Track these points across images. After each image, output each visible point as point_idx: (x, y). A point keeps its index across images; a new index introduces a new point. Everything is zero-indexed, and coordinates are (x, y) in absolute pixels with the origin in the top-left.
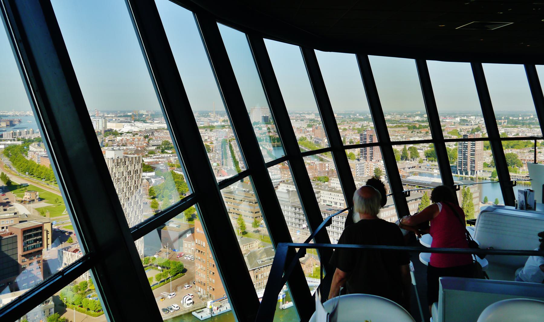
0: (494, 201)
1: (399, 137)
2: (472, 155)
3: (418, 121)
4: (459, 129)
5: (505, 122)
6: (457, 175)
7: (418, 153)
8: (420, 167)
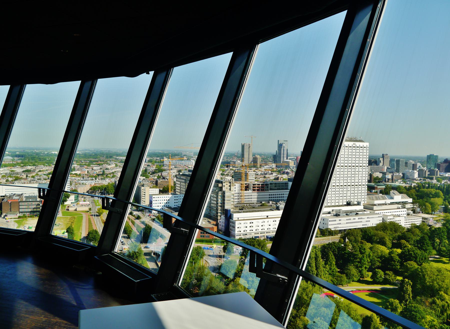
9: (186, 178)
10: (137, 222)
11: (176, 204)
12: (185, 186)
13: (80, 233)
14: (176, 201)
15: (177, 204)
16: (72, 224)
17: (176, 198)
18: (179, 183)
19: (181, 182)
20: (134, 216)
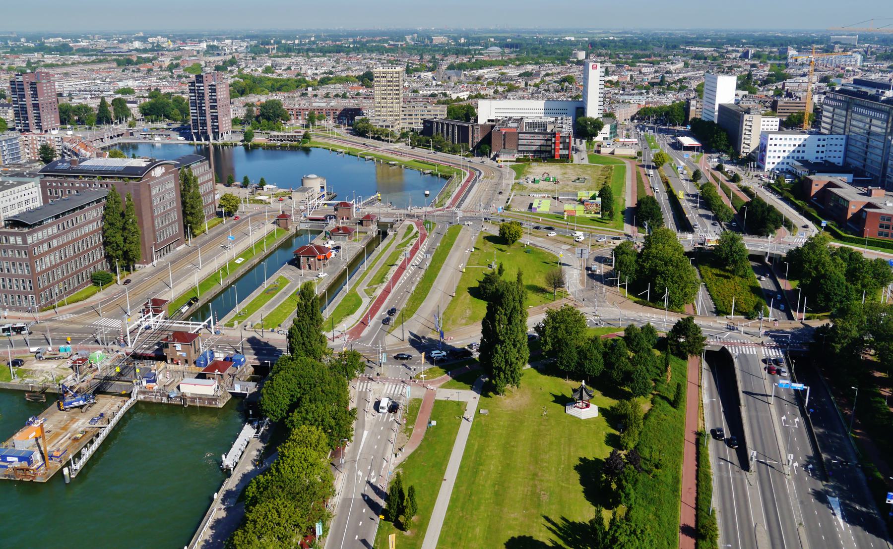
0: (243, 181)
1: (98, 81)
2: (212, 107)
3: (137, 50)
4: (203, 63)
5: (274, 48)
6: (192, 142)
7: (129, 110)
8: (132, 134)
9: (850, 98)
10: (733, 187)
11: (820, 155)
12: (846, 117)
13: (622, 200)
14: (821, 149)
15: (823, 155)
16: (608, 180)
17: (821, 143)
18: (831, 109)
19: (835, 107)
20: (725, 174)
